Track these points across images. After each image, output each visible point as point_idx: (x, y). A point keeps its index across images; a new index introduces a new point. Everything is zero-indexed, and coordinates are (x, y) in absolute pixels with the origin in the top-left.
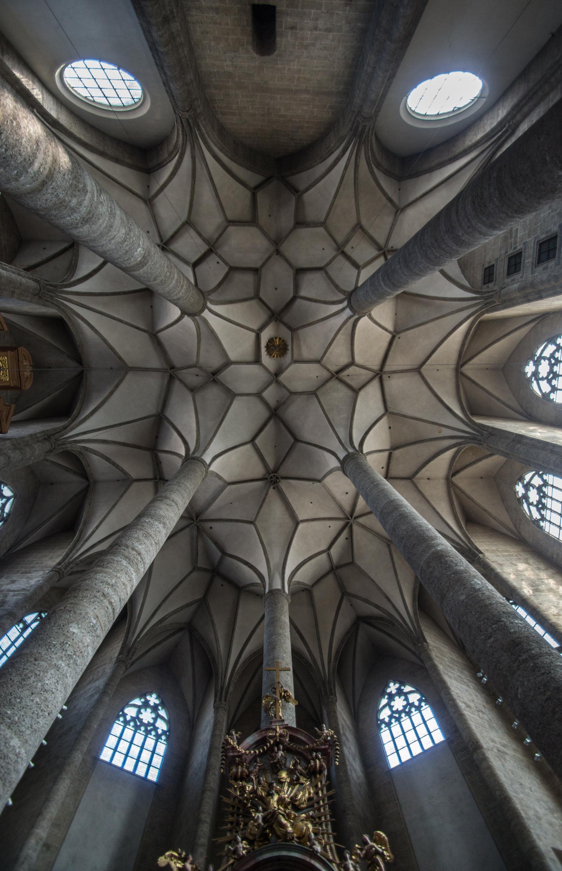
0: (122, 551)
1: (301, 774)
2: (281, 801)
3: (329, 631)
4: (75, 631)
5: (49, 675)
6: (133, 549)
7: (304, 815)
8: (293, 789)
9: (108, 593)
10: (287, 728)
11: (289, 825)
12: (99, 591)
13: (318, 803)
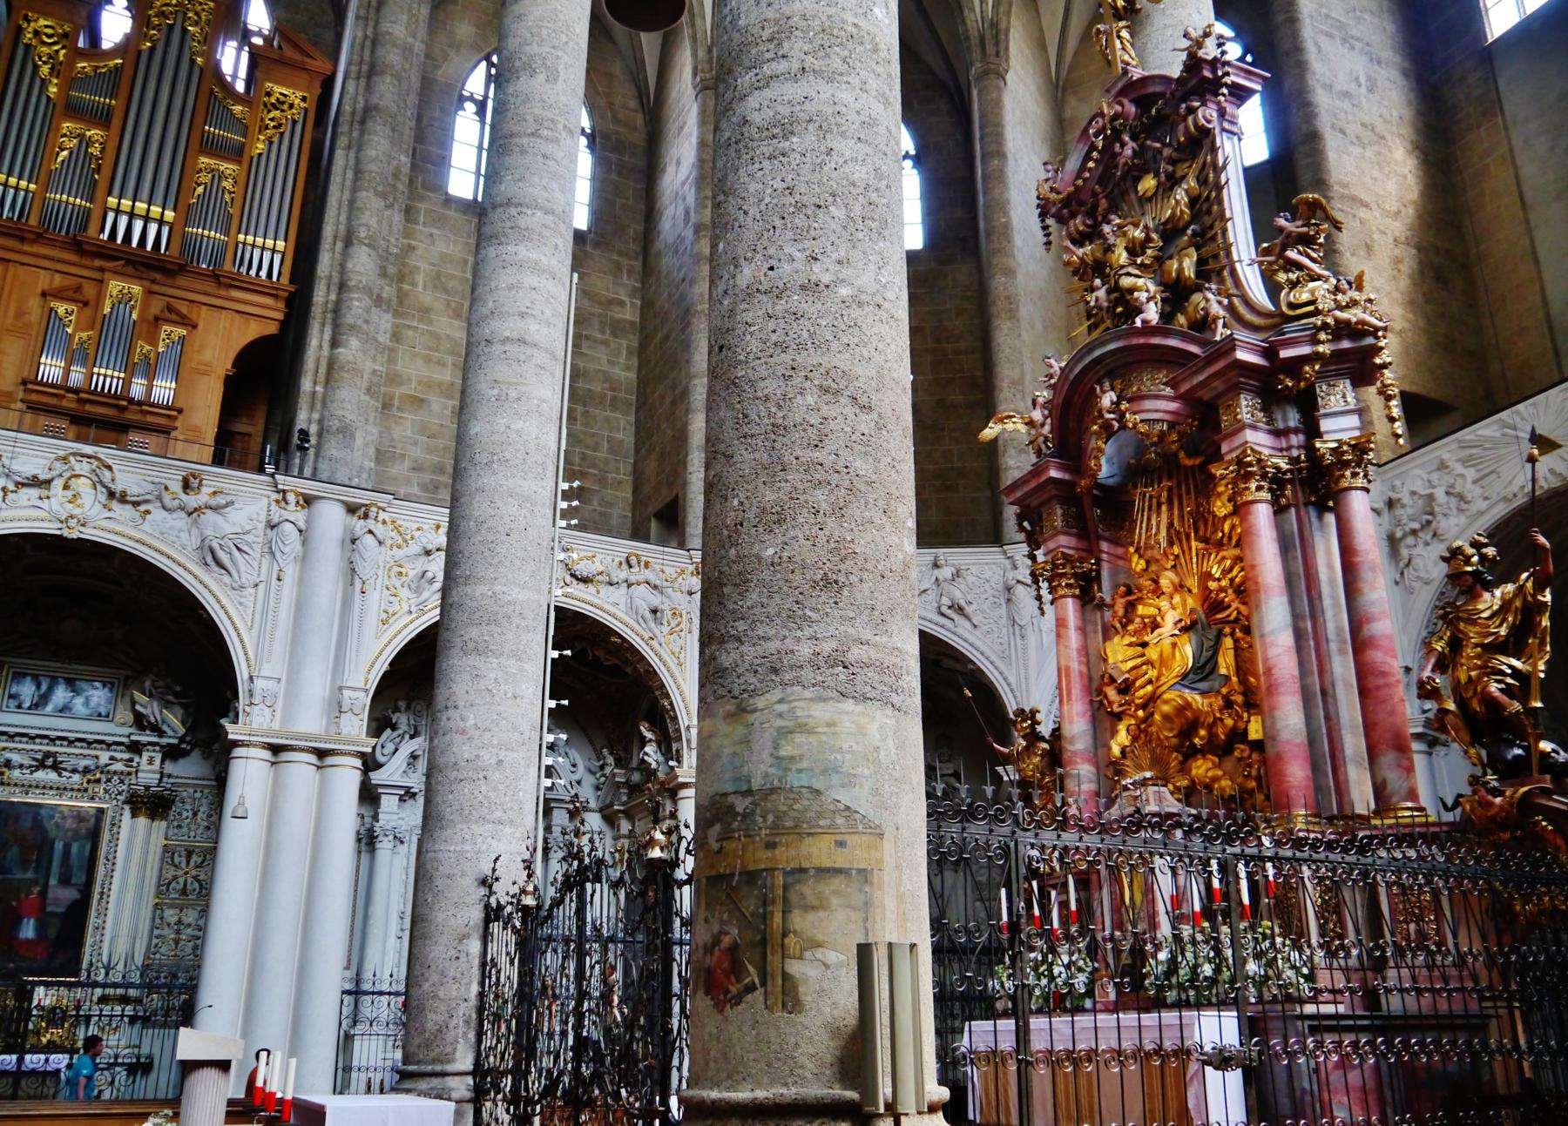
4: (477, 429)
5: (476, 505)
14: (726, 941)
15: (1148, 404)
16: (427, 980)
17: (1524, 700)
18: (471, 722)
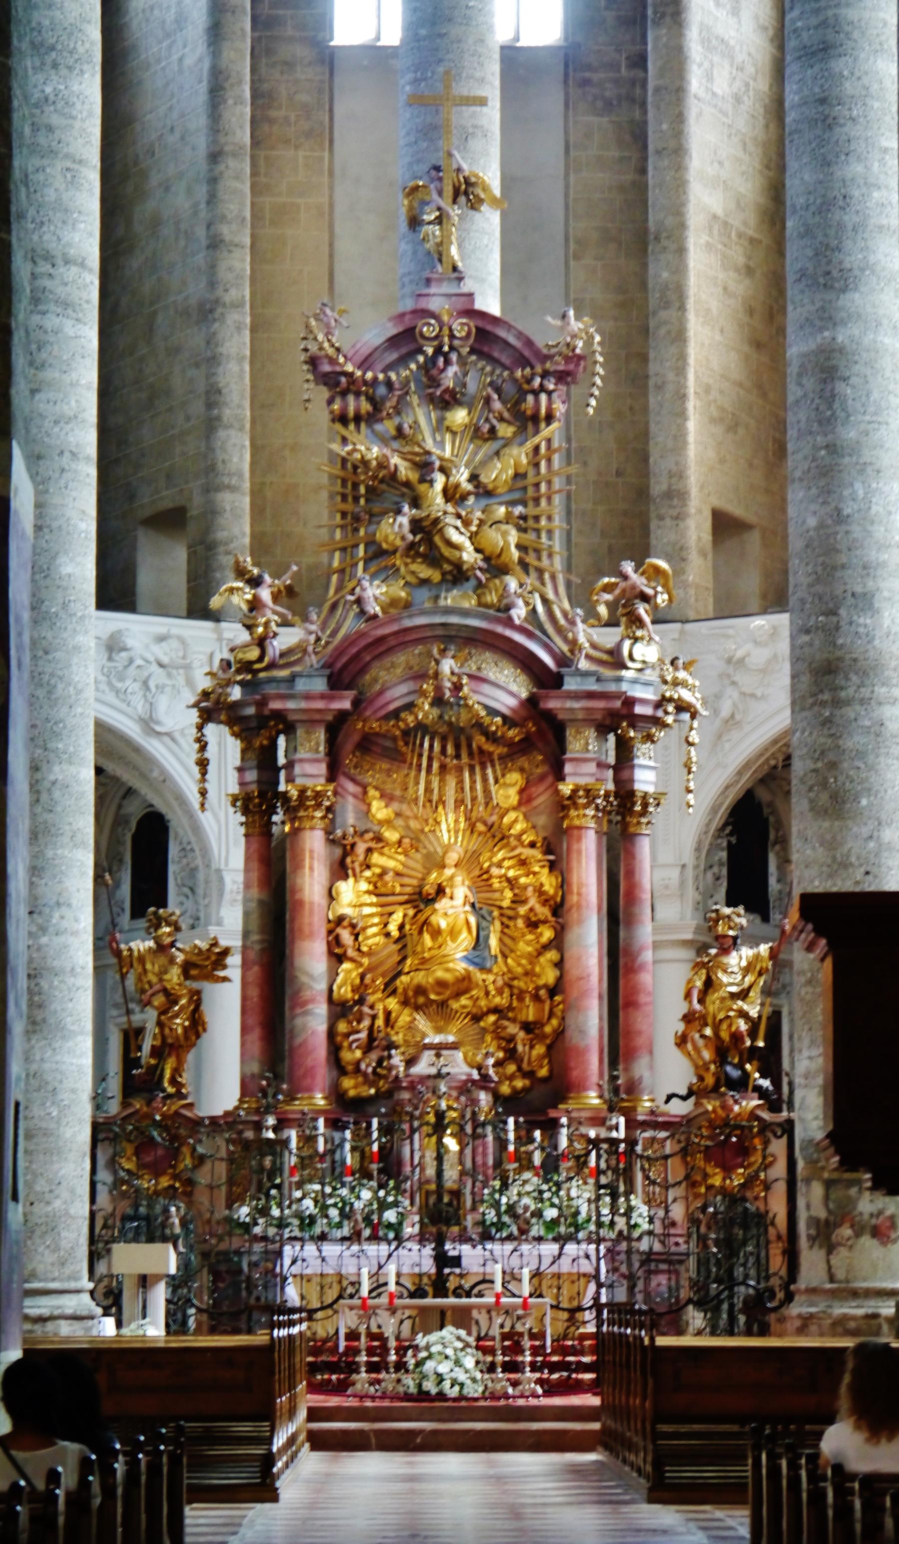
0: (47, 283)
1: (501, 419)
2: (451, 494)
5: (74, 668)
6: (67, 262)
7: (502, 510)
8: (479, 448)
9: (77, 445)
10: (471, 313)
11: (467, 544)
12: (62, 452)
13: (537, 485)
14: (888, 1213)
15: (486, 688)
16: (57, 1197)
18: (82, 925)
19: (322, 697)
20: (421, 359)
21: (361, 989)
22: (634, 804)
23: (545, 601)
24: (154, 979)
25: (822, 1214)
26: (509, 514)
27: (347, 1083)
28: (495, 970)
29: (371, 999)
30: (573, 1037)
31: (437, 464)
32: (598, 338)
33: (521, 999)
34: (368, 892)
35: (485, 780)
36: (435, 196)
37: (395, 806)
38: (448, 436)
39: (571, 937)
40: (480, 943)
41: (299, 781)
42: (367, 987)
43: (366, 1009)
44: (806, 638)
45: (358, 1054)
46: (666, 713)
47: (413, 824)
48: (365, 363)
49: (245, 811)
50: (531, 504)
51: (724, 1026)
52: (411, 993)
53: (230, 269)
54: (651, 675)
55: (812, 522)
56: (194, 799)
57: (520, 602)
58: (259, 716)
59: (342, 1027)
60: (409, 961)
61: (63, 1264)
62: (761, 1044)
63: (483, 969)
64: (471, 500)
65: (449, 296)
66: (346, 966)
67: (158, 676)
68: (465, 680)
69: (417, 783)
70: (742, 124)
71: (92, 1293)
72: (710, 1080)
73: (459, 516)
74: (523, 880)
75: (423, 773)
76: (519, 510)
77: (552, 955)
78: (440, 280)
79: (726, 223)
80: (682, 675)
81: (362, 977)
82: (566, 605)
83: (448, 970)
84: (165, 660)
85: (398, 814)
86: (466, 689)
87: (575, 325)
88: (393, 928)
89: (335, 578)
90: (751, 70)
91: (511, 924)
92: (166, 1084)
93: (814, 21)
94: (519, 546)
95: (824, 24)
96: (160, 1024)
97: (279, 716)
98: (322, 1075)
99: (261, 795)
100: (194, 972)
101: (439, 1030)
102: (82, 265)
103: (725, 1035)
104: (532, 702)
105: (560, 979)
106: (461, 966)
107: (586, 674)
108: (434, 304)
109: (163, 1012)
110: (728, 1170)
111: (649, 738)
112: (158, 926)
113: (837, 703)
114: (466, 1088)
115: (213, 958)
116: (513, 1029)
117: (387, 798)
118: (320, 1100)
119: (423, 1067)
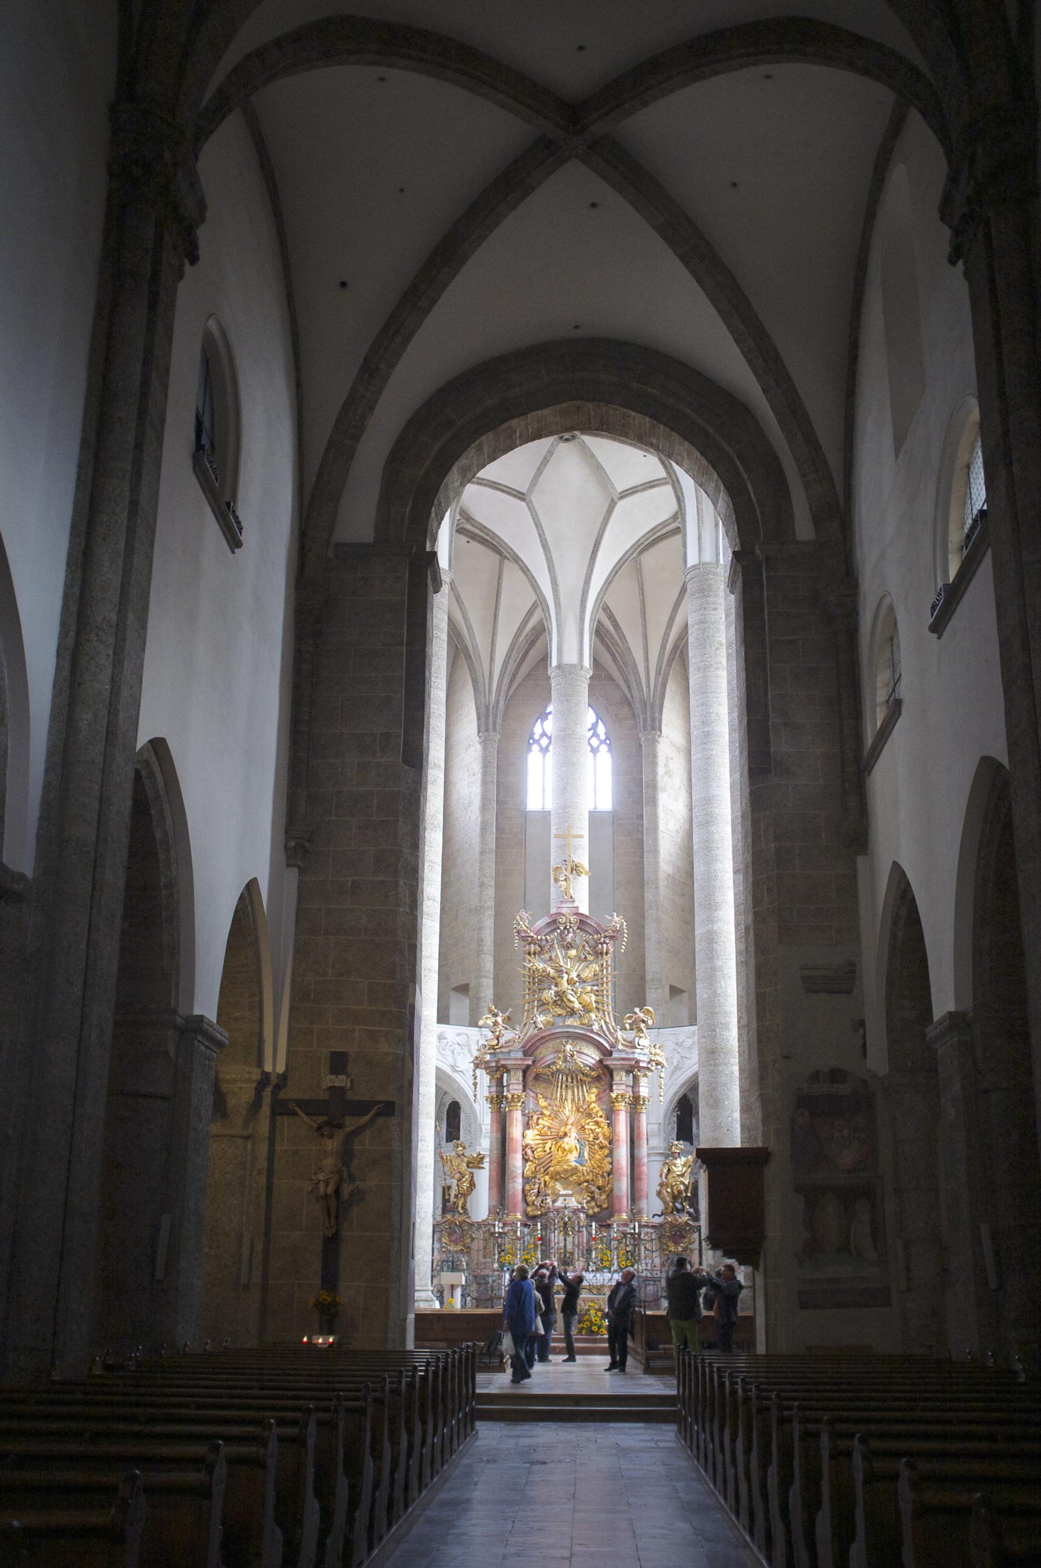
1: (589, 954)
2: (570, 982)
3: (665, 618)
6: (428, 899)
8: (580, 964)
10: (577, 914)
13: (602, 978)
15: (583, 1056)
16: (419, 1254)
17: (686, 1193)
19: (521, 1059)
20: (559, 931)
21: (535, 1172)
22: (640, 1101)
23: (606, 1022)
24: (456, 1168)
25: (712, 1262)
26: (592, 989)
27: (529, 1209)
28: (586, 1165)
29: (538, 1176)
30: (616, 1192)
31: (565, 970)
32: (625, 924)
33: (597, 1177)
34: (538, 1135)
35: (583, 1091)
36: (564, 871)
37: (548, 1101)
38: (569, 960)
39: (615, 1153)
40: (581, 1155)
41: (512, 1092)
42: (537, 1172)
43: (537, 1180)
44: (704, 1040)
45: (534, 1198)
46: (652, 1066)
47: (555, 1108)
48: (537, 933)
49: (491, 1103)
50: (600, 985)
51: (675, 1188)
52: (554, 1174)
53: (487, 895)
54: (646, 1051)
55: (705, 996)
56: (472, 1098)
57: (596, 1023)
58: (496, 1066)
59: (527, 1187)
60: (553, 1162)
61: (421, 1280)
62: (689, 1195)
63: (582, 1165)
64: (578, 984)
65: (569, 907)
66: (529, 1163)
67: (458, 1049)
68: (575, 1053)
69: (557, 1092)
70: (679, 840)
71: (432, 1291)
72: (670, 1210)
73: (573, 990)
74: (597, 1130)
75: (559, 1089)
76: (595, 988)
77: (609, 1159)
78: (566, 902)
79: (674, 878)
80: (658, 1051)
81: (535, 1168)
82: (614, 1024)
83: (569, 1165)
84: (461, 1043)
85: (549, 1104)
86: (575, 1057)
87: (616, 919)
88: (547, 1148)
89: (526, 1013)
90: (682, 821)
91: (593, 1147)
92: (460, 1209)
93: (703, 813)
94: (595, 1002)
95: (707, 814)
96: (458, 1186)
97: (504, 1066)
98: (520, 1205)
99: (497, 1097)
100: (471, 1165)
101: (565, 1189)
102: (435, 900)
103: (676, 1192)
104: (601, 1061)
105: (612, 1169)
106: (574, 1164)
107: (621, 1051)
108: (564, 911)
109: (459, 1180)
110: (676, 1244)
111: (645, 1075)
112: (457, 1147)
113: (715, 1065)
114: (576, 1211)
115: (479, 1160)
116: (593, 1188)
117: (545, 1098)
118: (519, 1216)
119: (559, 1203)
